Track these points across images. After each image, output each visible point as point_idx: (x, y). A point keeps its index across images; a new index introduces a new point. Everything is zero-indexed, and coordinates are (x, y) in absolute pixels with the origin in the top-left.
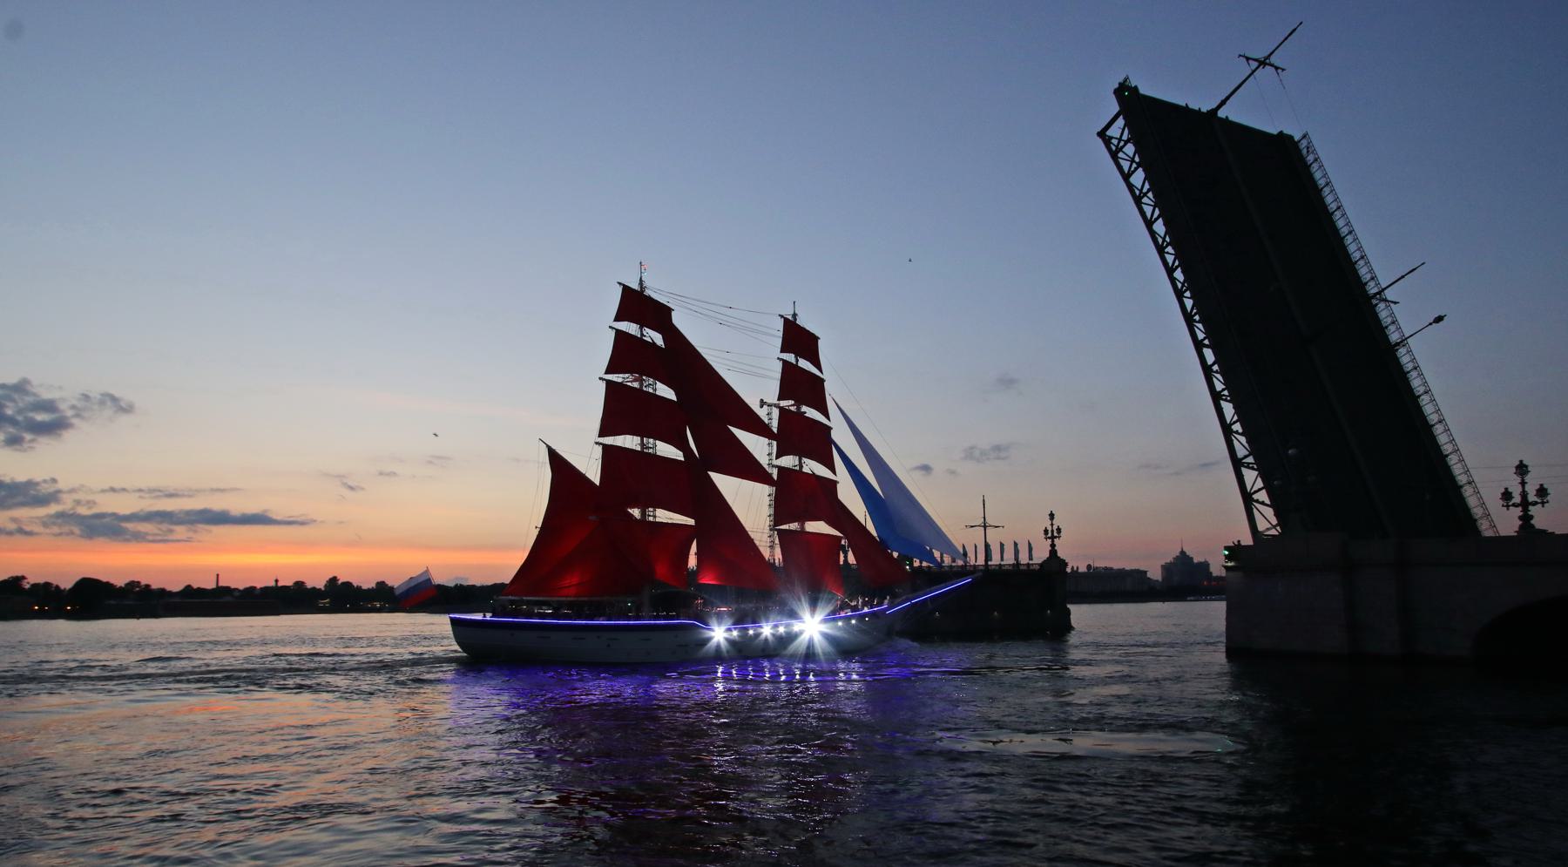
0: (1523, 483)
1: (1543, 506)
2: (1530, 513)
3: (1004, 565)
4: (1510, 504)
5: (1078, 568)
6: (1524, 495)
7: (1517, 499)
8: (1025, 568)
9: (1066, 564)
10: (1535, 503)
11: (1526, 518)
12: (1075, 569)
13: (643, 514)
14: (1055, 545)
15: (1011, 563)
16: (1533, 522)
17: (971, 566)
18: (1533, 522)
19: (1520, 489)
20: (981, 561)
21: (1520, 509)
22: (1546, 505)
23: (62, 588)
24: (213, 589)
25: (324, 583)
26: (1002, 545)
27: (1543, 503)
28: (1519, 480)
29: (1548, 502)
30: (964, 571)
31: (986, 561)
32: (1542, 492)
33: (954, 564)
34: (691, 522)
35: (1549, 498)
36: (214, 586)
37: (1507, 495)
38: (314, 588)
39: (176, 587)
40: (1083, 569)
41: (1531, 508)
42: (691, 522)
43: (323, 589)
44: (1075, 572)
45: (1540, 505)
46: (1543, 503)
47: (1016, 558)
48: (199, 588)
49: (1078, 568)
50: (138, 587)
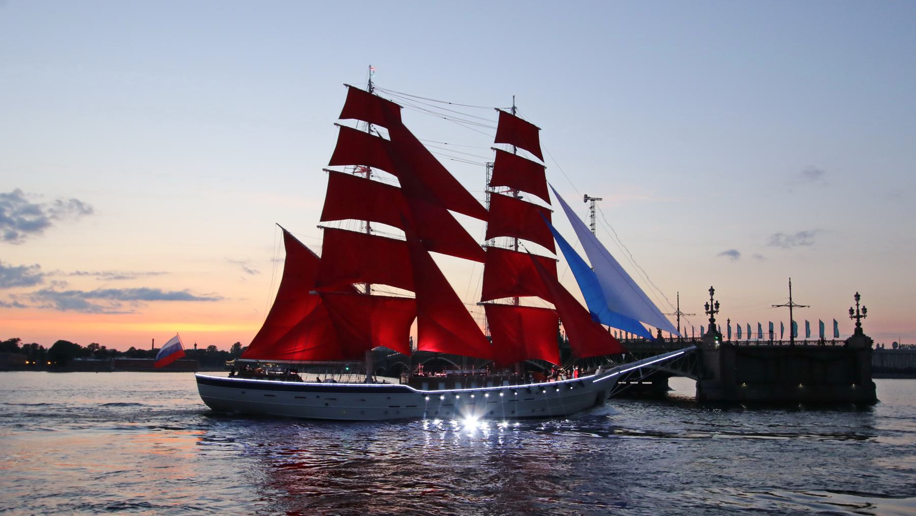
0: (858, 305)
2: (860, 322)
3: (809, 342)
5: (883, 345)
6: (858, 311)
7: (855, 314)
8: (830, 344)
9: (872, 342)
10: (862, 316)
11: (858, 324)
12: (881, 346)
13: (368, 289)
14: (860, 324)
15: (817, 340)
17: (776, 342)
20: (787, 337)
21: (856, 319)
22: (866, 317)
23: (45, 348)
24: (150, 351)
25: (186, 349)
26: (807, 324)
28: (856, 303)
30: (672, 345)
31: (792, 337)
33: (760, 340)
34: (411, 295)
35: (867, 314)
36: (151, 349)
37: (851, 311)
38: (120, 352)
39: (124, 349)
40: (888, 346)
41: (860, 319)
42: (411, 295)
43: (230, 352)
44: (880, 350)
46: (865, 316)
47: (822, 335)
48: (140, 350)
49: (883, 345)
50: (97, 348)
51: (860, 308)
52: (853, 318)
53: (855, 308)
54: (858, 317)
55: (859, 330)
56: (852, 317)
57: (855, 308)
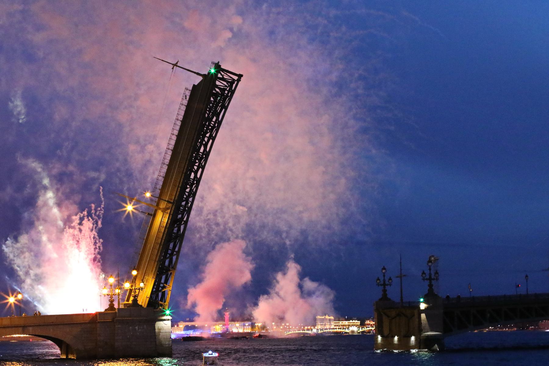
1: (390, 286)
2: (386, 289)
11: (385, 291)
19: (383, 278)
21: (383, 286)
27: (390, 285)
41: (386, 287)
45: (389, 286)
54: (384, 285)
56: (424, 279)
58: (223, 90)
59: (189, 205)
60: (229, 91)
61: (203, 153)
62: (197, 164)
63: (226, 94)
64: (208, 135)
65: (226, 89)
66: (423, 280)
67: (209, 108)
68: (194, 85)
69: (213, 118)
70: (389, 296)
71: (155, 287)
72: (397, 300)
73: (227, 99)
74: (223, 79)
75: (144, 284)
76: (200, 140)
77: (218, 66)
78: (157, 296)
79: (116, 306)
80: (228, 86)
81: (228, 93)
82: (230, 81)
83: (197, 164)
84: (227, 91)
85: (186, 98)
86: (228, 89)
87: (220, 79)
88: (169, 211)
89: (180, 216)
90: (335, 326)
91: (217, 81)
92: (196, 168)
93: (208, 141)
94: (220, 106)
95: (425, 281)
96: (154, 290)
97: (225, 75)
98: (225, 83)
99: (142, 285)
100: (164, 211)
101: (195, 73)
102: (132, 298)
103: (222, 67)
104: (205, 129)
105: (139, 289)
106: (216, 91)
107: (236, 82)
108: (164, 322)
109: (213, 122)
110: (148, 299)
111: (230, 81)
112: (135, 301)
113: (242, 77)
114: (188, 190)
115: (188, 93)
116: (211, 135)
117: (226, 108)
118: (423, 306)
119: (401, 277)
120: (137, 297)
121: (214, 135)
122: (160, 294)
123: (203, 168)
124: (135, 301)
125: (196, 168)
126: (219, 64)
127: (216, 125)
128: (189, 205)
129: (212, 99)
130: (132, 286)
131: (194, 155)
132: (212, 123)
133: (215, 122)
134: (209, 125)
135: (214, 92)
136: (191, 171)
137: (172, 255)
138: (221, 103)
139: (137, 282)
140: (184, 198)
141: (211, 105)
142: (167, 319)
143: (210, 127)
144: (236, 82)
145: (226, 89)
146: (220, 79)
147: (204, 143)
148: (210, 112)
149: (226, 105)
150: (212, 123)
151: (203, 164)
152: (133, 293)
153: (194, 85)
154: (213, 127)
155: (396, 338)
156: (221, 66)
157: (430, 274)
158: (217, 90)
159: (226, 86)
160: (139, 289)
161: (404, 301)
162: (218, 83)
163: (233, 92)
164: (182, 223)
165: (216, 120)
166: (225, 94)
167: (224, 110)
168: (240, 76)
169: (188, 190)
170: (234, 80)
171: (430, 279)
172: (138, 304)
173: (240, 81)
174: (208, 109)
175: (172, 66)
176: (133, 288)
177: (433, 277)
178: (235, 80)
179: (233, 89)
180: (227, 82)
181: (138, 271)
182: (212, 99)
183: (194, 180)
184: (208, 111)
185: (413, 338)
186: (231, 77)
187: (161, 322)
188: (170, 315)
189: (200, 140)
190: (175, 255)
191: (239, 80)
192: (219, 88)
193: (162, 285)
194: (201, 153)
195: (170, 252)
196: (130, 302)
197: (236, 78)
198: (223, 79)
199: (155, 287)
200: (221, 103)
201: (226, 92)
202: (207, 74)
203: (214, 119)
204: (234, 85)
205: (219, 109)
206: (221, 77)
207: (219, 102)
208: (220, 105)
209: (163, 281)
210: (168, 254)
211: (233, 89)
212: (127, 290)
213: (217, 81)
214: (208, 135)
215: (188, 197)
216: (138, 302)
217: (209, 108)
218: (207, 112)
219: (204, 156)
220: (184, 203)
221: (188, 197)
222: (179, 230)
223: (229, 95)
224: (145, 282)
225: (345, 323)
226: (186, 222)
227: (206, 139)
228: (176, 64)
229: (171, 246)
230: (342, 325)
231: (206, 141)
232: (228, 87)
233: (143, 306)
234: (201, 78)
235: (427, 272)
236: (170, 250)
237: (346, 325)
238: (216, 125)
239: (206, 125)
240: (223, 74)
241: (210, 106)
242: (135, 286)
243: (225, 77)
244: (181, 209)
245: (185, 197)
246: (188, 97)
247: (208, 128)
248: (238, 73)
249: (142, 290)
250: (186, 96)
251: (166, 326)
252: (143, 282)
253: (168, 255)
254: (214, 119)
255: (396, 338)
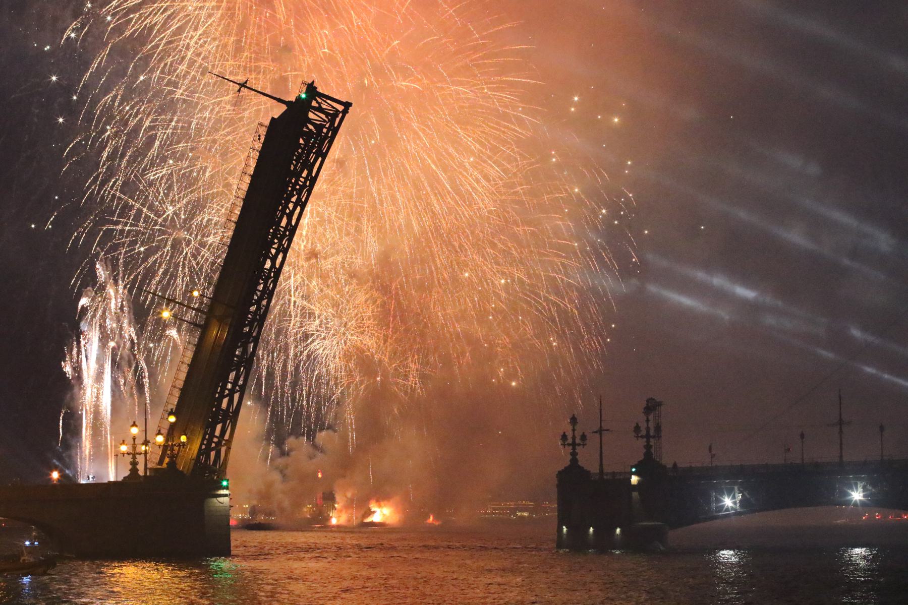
2: (576, 451)
4: (566, 443)
6: (574, 438)
10: (579, 445)
11: (574, 454)
16: (577, 457)
18: (577, 457)
21: (571, 447)
22: (585, 447)
29: (586, 445)
32: (584, 437)
35: (587, 442)
41: (577, 447)
46: (584, 445)
51: (578, 434)
52: (566, 446)
53: (569, 434)
55: (574, 460)
57: (569, 434)
58: (319, 127)
59: (262, 311)
60: (329, 129)
61: (286, 228)
62: (275, 246)
63: (324, 133)
64: (294, 199)
65: (324, 126)
66: (636, 438)
67: (296, 156)
68: (273, 118)
69: (302, 172)
70: (580, 463)
71: (205, 442)
72: (594, 469)
73: (327, 141)
74: (320, 109)
75: (187, 438)
76: (281, 207)
77: (311, 89)
78: (208, 457)
79: (141, 472)
80: (327, 120)
81: (328, 132)
82: (332, 112)
83: (275, 246)
84: (326, 128)
85: (259, 139)
86: (327, 126)
87: (315, 108)
88: (229, 320)
89: (247, 329)
90: (494, 509)
91: (310, 113)
92: (273, 251)
93: (295, 208)
94: (314, 153)
95: (640, 439)
96: (203, 447)
97: (323, 102)
98: (323, 116)
99: (183, 438)
100: (221, 320)
101: (275, 98)
102: (167, 460)
103: (320, 90)
104: (290, 189)
105: (179, 445)
106: (308, 128)
107: (341, 115)
108: (218, 499)
109: (303, 178)
110: (193, 462)
111: (332, 112)
112: (172, 464)
113: (351, 106)
114: (261, 287)
115: (263, 131)
116: (299, 199)
117: (324, 156)
118: (634, 479)
119: (600, 431)
120: (176, 458)
121: (303, 200)
122: (213, 454)
123: (285, 252)
124: (172, 464)
125: (273, 251)
126: (315, 85)
127: (308, 184)
128: (262, 311)
129: (301, 141)
130: (167, 440)
131: (271, 231)
132: (301, 179)
133: (306, 179)
134: (296, 183)
135: (304, 129)
136: (266, 257)
137: (232, 392)
138: (316, 147)
139: (176, 434)
140: (255, 300)
141: (300, 151)
142: (223, 494)
143: (298, 187)
144: (341, 115)
145: (324, 126)
146: (315, 108)
147: (288, 211)
148: (298, 162)
149: (324, 151)
150: (301, 179)
151: (285, 246)
152: (169, 452)
153: (273, 118)
154: (303, 187)
155: (591, 530)
156: (316, 88)
157: (648, 429)
158: (311, 127)
159: (325, 121)
160: (179, 445)
161: (605, 471)
162: (311, 115)
163: (335, 131)
164: (250, 340)
165: (308, 175)
166: (323, 134)
167: (320, 159)
168: (347, 105)
169: (261, 287)
170: (337, 111)
171: (648, 436)
172: (178, 470)
173: (348, 112)
174: (295, 158)
175: (238, 87)
176: (170, 443)
177: (652, 433)
178: (339, 111)
179: (336, 125)
180: (327, 114)
181: (177, 417)
182: (301, 141)
183: (270, 270)
184: (294, 160)
185: (618, 530)
186: (333, 107)
187: (215, 499)
188: (227, 488)
189: (281, 207)
190: (237, 392)
191: (345, 112)
192: (313, 124)
193: (215, 440)
194: (282, 227)
195: (229, 386)
196: (165, 465)
197: (340, 108)
198: (320, 109)
199: (205, 442)
200: (316, 147)
201: (325, 130)
202: (294, 100)
203: (304, 174)
204: (338, 120)
205: (312, 157)
206: (317, 105)
207: (313, 147)
208: (314, 151)
209: (217, 433)
210: (228, 389)
211: (336, 125)
212: (160, 446)
213: (310, 113)
214: (294, 199)
215: (261, 299)
216: (178, 466)
217: (296, 156)
218: (294, 162)
219: (287, 233)
220: (253, 308)
221: (261, 299)
222: (245, 350)
223: (329, 135)
224: (189, 434)
225: (510, 505)
226: (256, 341)
227: (291, 206)
228: (244, 84)
229: (232, 375)
230: (503, 509)
231: (291, 208)
232: (327, 123)
233: (185, 472)
234: (284, 108)
235: (643, 426)
236: (230, 382)
237: (510, 509)
238: (308, 184)
239: (292, 183)
240: (320, 100)
241: (298, 152)
242: (173, 441)
243: (324, 107)
244: (249, 318)
245: (256, 298)
246: (262, 140)
247: (294, 189)
248: (344, 101)
249: (183, 447)
250: (259, 136)
251: (221, 505)
252: (185, 434)
253: (227, 392)
254: (304, 174)
255: (591, 530)
